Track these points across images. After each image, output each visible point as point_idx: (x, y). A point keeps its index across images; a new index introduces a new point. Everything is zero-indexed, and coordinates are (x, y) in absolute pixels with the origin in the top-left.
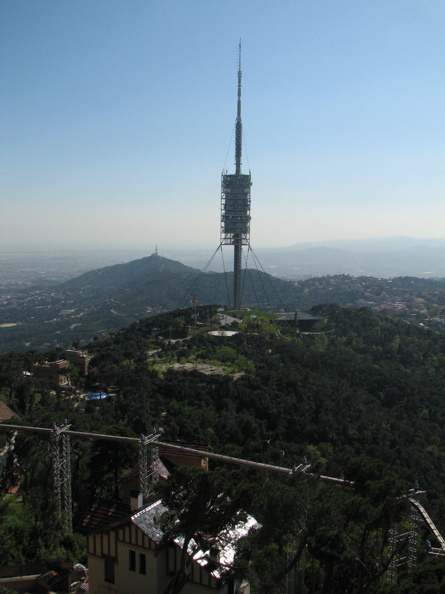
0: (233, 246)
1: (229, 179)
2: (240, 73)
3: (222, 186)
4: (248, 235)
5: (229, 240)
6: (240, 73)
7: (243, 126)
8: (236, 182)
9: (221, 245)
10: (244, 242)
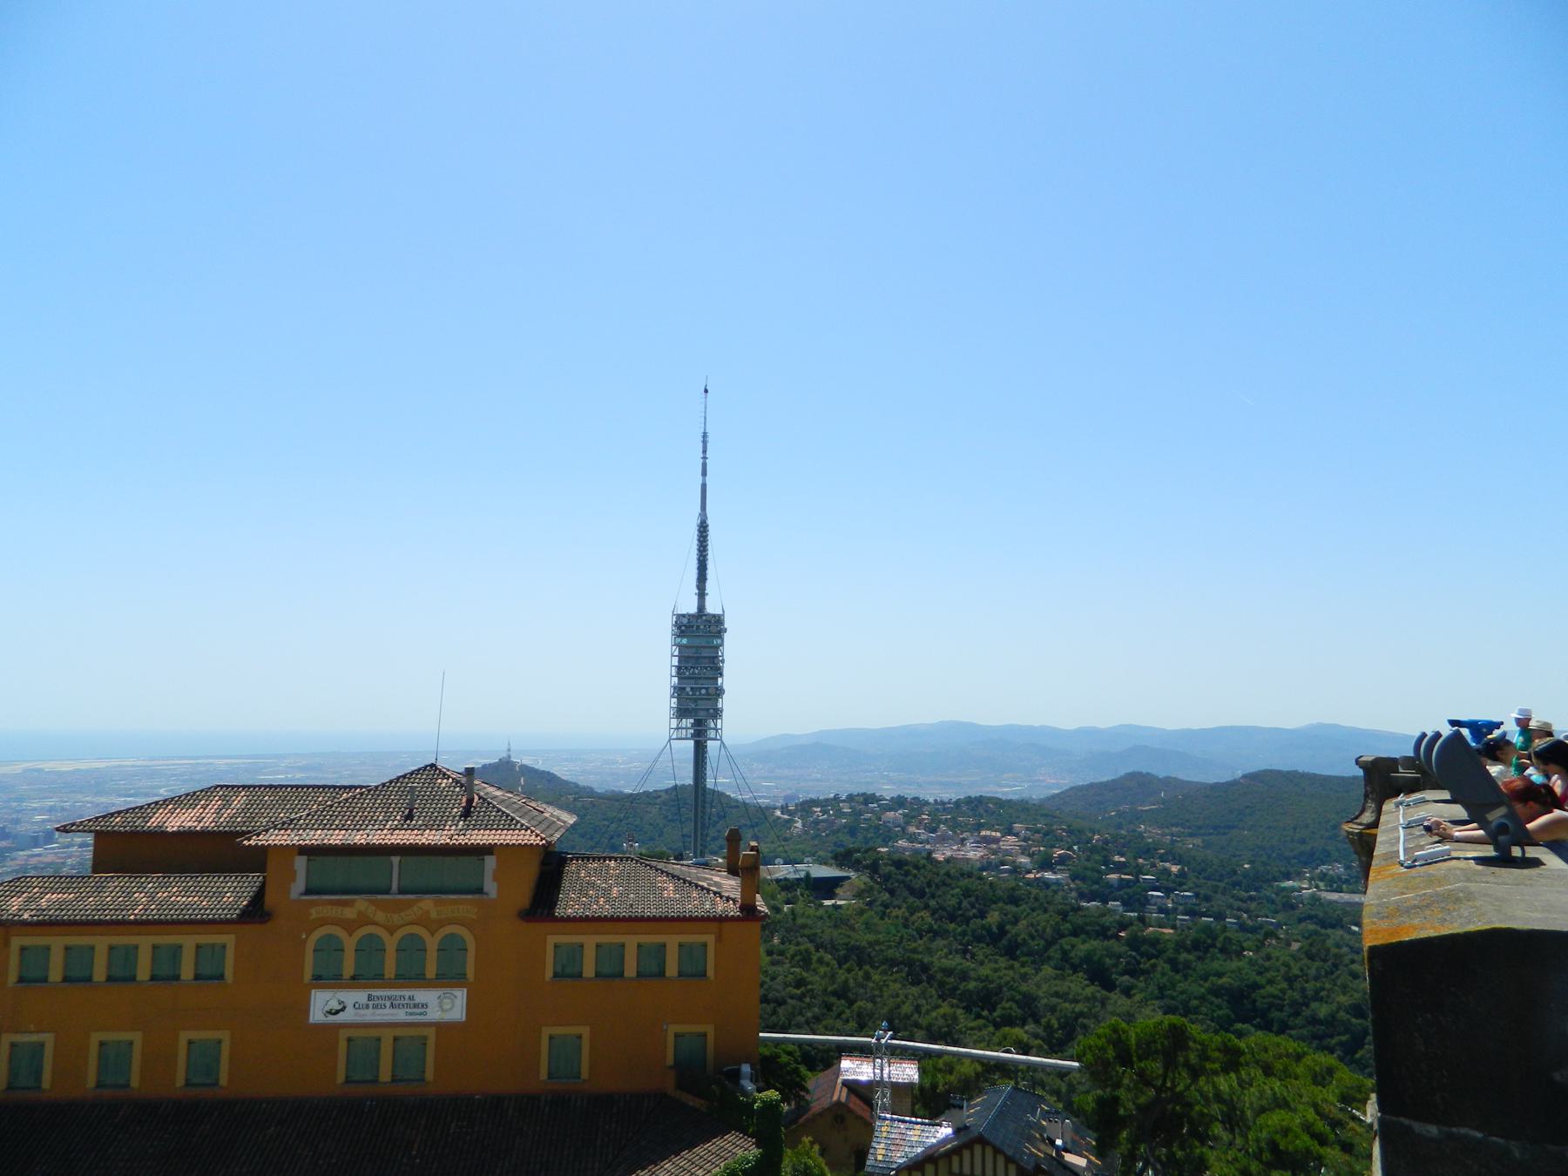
1: (685, 621)
2: (705, 435)
6: (705, 435)
7: (710, 528)
10: (712, 734)
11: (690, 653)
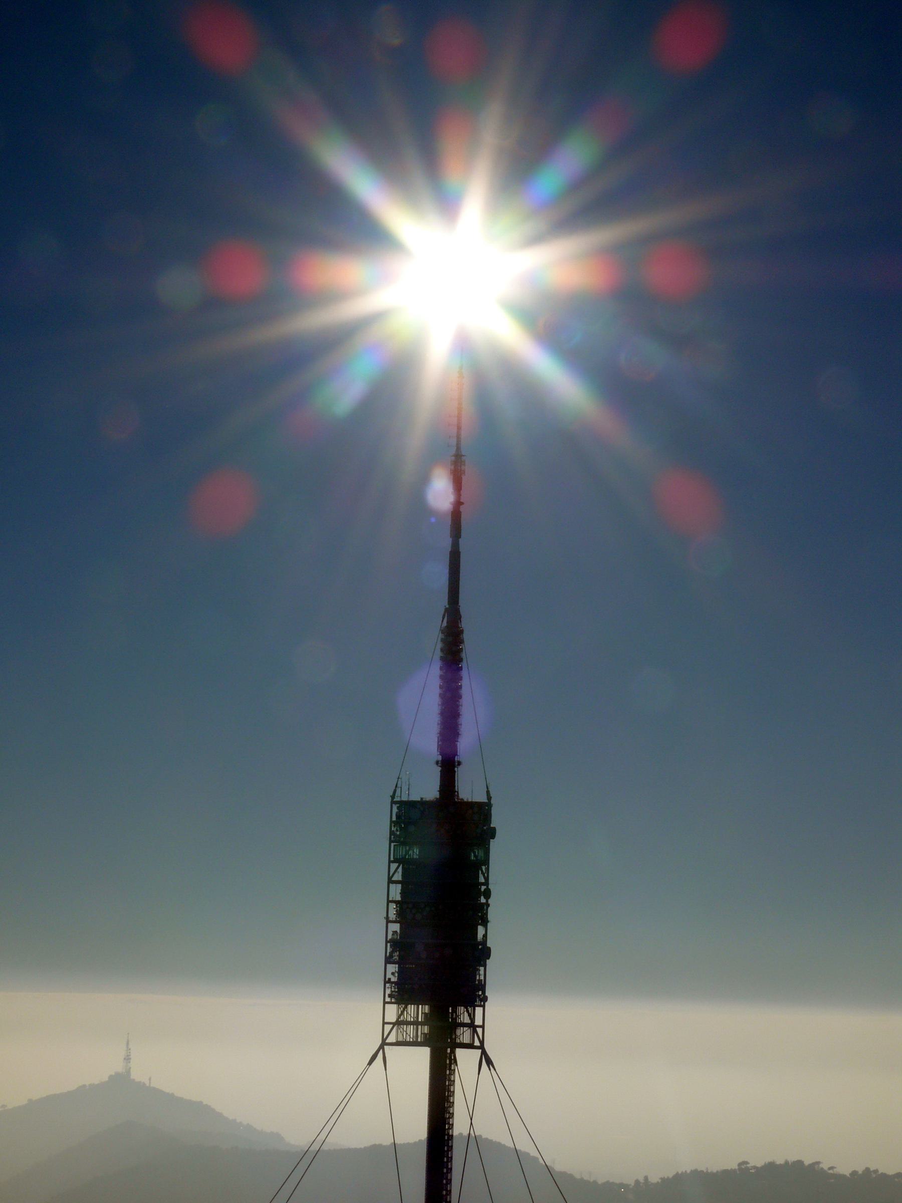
3: (394, 838)
4: (479, 1010)
5: (411, 1028)
7: (466, 636)
9: (382, 1047)
10: (465, 1035)
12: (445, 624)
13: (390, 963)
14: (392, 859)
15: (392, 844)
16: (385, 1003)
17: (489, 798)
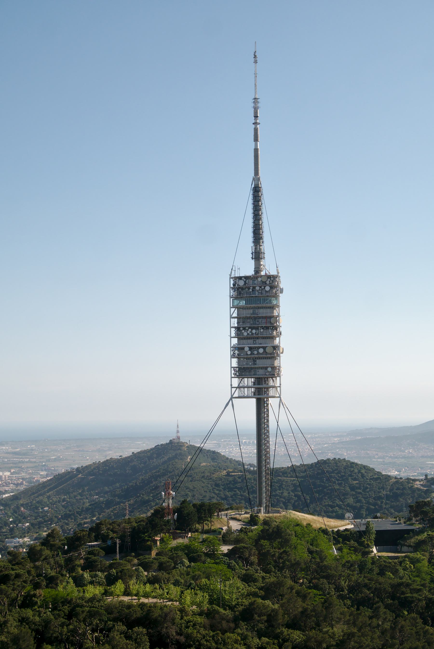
0: (254, 401)
1: (241, 283)
4: (278, 378)
5: (246, 389)
8: (254, 288)
9: (231, 399)
10: (271, 392)
11: (247, 313)
12: (253, 186)
13: (233, 358)
14: (231, 306)
15: (231, 299)
16: (232, 377)
17: (278, 273)
